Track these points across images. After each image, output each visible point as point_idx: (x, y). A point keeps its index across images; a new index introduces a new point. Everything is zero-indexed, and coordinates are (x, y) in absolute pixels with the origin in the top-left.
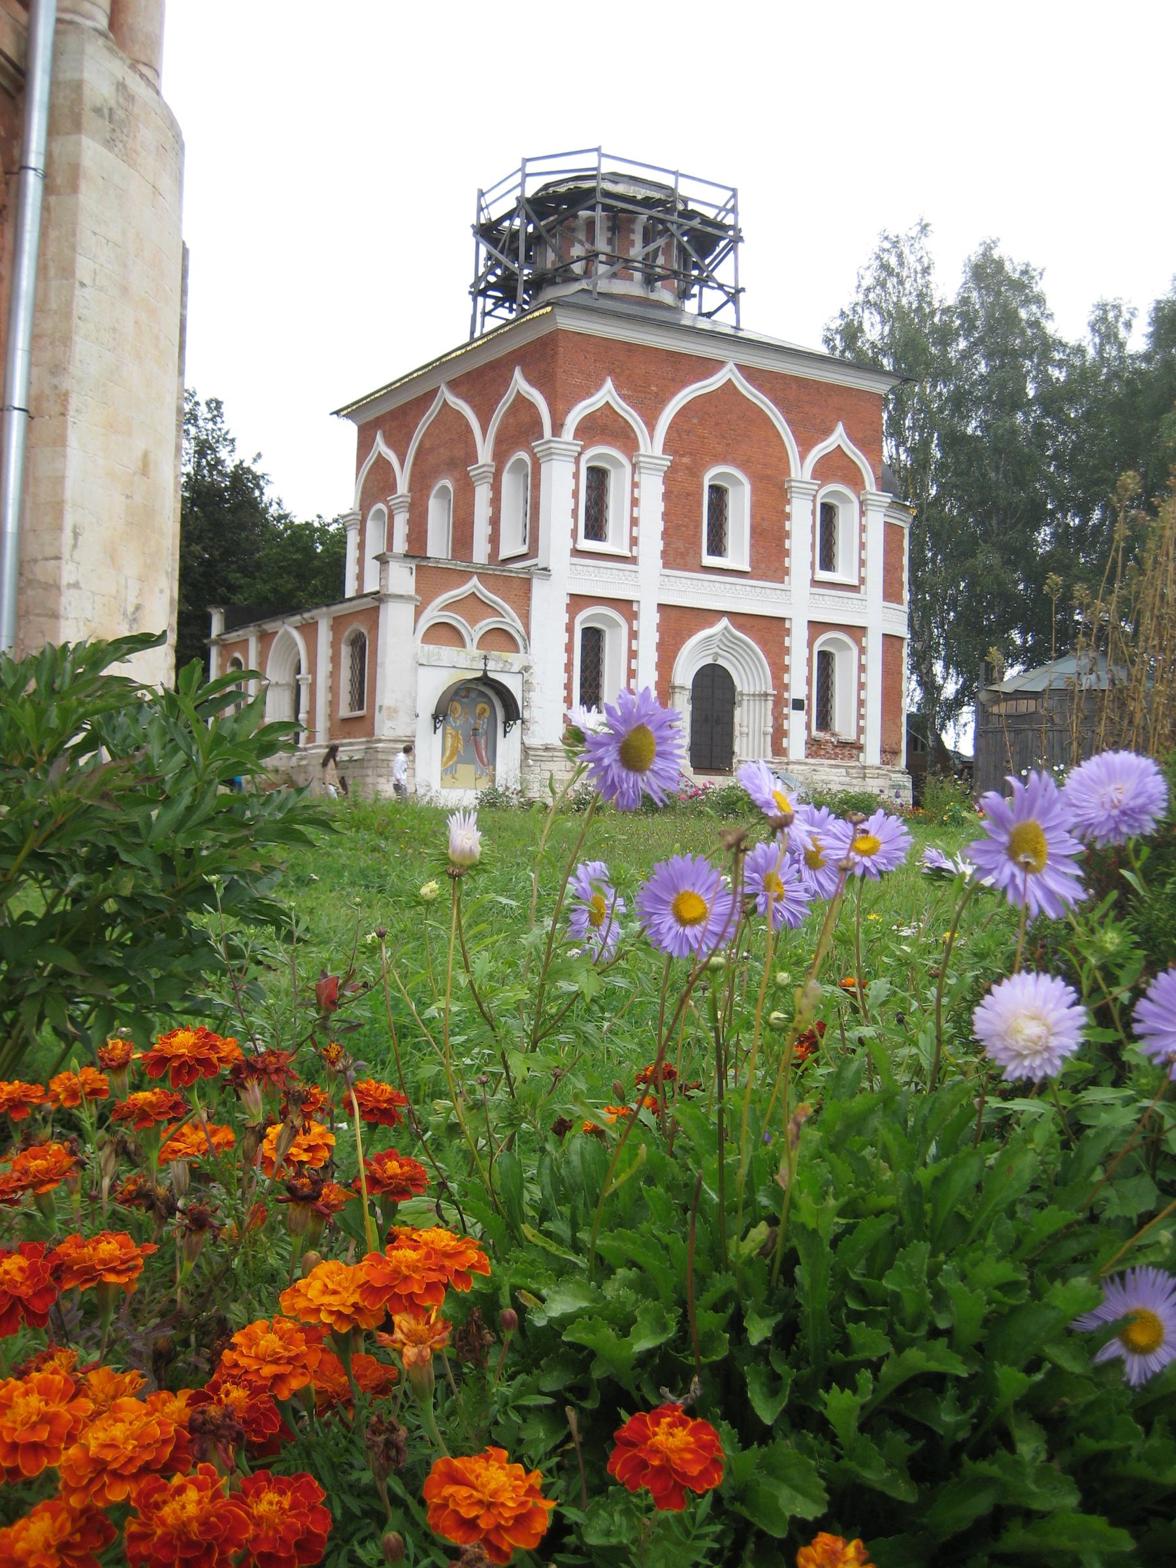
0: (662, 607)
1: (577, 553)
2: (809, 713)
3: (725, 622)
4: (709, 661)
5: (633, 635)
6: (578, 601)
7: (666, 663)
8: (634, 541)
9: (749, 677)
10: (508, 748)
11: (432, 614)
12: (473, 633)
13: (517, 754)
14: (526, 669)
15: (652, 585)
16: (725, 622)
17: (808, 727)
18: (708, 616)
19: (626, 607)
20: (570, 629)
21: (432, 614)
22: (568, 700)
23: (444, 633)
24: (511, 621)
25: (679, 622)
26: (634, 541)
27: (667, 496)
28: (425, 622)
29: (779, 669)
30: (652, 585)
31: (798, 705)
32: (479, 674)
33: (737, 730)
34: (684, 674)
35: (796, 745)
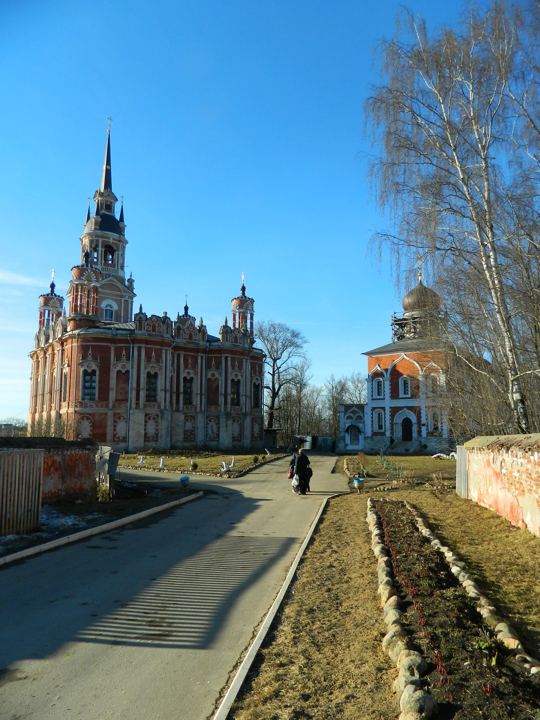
0: (390, 407)
1: (372, 399)
2: (427, 426)
3: (405, 409)
4: (405, 417)
5: (385, 414)
6: (374, 409)
7: (392, 419)
8: (384, 395)
9: (413, 418)
10: (361, 437)
11: (348, 414)
12: (354, 418)
13: (363, 438)
14: (364, 422)
15: (388, 403)
16: (405, 409)
17: (427, 429)
18: (401, 408)
19: (383, 409)
20: (372, 414)
21: (348, 414)
22: (372, 427)
23: (349, 417)
24: (362, 415)
25: (394, 411)
26: (384, 395)
27: (390, 385)
28: (346, 416)
29: (419, 417)
30: (388, 403)
31: (424, 425)
32: (350, 424)
33: (413, 431)
34: (399, 419)
35: (424, 434)
